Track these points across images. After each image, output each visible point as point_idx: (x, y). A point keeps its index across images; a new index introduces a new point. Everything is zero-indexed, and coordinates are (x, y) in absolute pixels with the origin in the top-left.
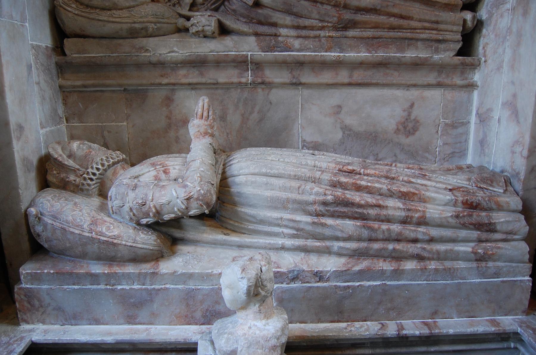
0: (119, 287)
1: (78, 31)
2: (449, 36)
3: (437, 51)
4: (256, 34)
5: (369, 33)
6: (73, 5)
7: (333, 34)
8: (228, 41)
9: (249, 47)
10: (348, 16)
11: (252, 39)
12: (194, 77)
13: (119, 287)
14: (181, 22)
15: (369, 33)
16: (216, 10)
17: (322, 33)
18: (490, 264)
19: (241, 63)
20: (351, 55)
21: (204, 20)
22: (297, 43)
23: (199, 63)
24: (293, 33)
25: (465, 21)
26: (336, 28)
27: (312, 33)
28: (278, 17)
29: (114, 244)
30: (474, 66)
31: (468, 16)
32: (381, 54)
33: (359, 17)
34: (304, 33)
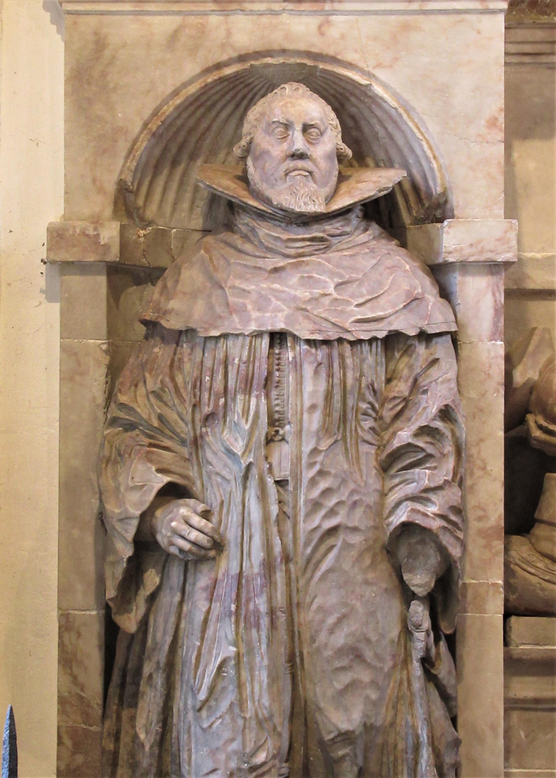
1: (540, 607)
6: (540, 565)
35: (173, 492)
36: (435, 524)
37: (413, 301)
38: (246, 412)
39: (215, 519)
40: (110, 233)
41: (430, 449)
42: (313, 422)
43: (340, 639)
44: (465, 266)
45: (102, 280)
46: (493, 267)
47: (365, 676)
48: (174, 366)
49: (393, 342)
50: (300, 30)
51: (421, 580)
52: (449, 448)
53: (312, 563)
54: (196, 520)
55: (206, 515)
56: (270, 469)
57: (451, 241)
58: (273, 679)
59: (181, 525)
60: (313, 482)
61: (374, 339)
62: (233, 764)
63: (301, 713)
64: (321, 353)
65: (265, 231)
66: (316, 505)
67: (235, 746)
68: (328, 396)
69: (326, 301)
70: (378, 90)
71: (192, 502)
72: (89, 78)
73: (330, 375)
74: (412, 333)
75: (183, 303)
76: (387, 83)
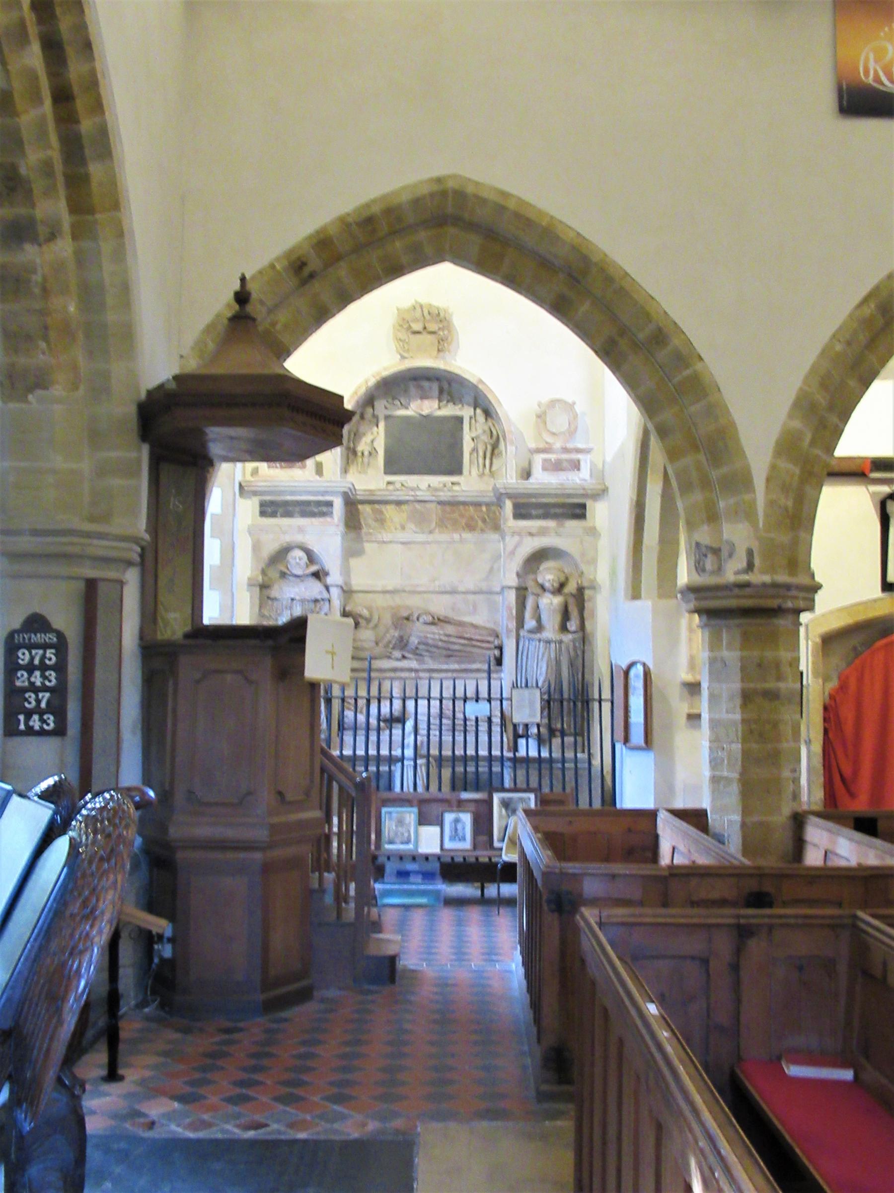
9: (414, 664)
10: (450, 653)
12: (392, 675)
19: (411, 670)
21: (397, 654)
23: (395, 670)
30: (501, 671)
32: (463, 666)
33: (455, 653)
37: (321, 592)
40: (260, 578)
44: (332, 586)
45: (258, 589)
46: (337, 586)
48: (272, 605)
49: (316, 601)
50: (299, 538)
57: (329, 580)
65: (291, 578)
72: (256, 547)
75: (274, 593)
76: (316, 549)
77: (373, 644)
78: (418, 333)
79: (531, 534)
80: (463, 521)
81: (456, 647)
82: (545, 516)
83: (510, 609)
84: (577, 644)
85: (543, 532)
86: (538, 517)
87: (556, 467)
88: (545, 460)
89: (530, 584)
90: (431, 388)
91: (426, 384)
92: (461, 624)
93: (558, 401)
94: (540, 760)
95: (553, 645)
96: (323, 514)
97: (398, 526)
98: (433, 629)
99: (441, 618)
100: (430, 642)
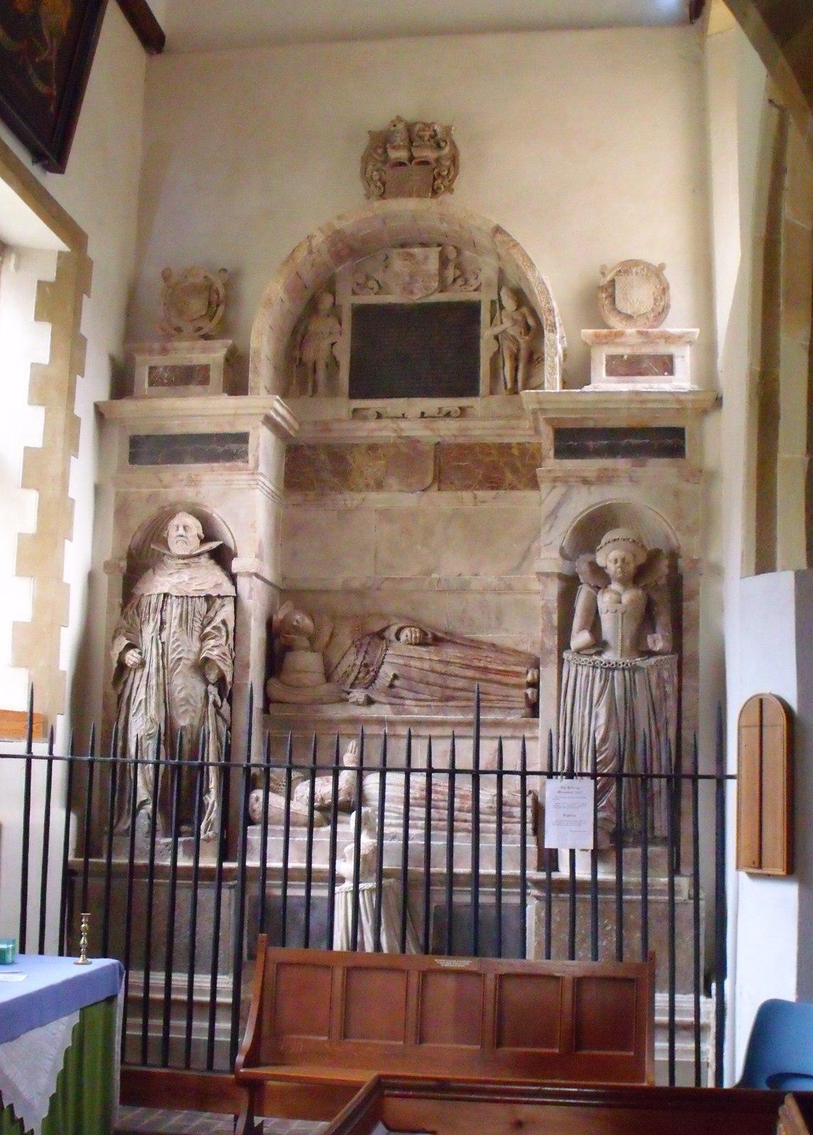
0: (297, 839)
2: (516, 705)
3: (509, 714)
4: (391, 704)
5: (463, 703)
7: (439, 704)
8: (374, 708)
10: (448, 692)
11: (388, 706)
13: (297, 839)
14: (344, 695)
15: (463, 703)
16: (367, 688)
17: (432, 704)
18: (510, 836)
19: (381, 722)
20: (451, 717)
22: (416, 710)
24: (414, 703)
25: (527, 695)
26: (441, 701)
27: (426, 703)
28: (404, 693)
29: (297, 814)
31: (529, 691)
34: (422, 703)
35: (130, 646)
36: (215, 658)
38: (153, 619)
39: (143, 655)
41: (217, 634)
42: (175, 623)
43: (182, 695)
46: (250, 575)
47: (190, 708)
49: (208, 598)
50: (190, 494)
51: (212, 677)
52: (224, 633)
53: (173, 670)
54: (136, 655)
55: (140, 654)
56: (160, 638)
57: (236, 565)
58: (158, 706)
59: (132, 658)
60: (174, 643)
61: (199, 597)
62: (142, 733)
63: (169, 720)
64: (180, 600)
66: (174, 650)
67: (143, 727)
68: (181, 615)
69: (184, 584)
70: (214, 515)
71: (136, 649)
73: (182, 607)
74: (214, 595)
76: (218, 513)
77: (319, 677)
78: (402, 164)
79: (585, 481)
80: (480, 474)
81: (461, 683)
82: (612, 452)
83: (549, 614)
84: (666, 674)
85: (605, 478)
86: (598, 453)
87: (629, 366)
88: (611, 359)
89: (582, 568)
90: (426, 258)
91: (416, 251)
92: (474, 645)
93: (636, 263)
94: (595, 885)
95: (617, 675)
96: (230, 456)
97: (372, 483)
98: (422, 651)
99: (440, 635)
100: (415, 674)
